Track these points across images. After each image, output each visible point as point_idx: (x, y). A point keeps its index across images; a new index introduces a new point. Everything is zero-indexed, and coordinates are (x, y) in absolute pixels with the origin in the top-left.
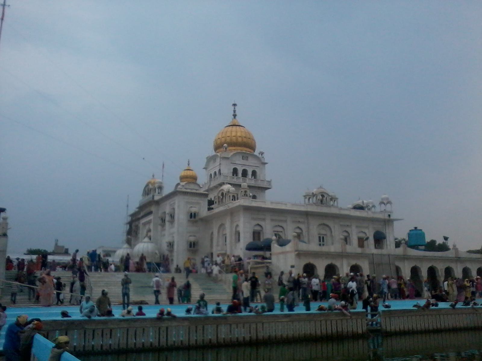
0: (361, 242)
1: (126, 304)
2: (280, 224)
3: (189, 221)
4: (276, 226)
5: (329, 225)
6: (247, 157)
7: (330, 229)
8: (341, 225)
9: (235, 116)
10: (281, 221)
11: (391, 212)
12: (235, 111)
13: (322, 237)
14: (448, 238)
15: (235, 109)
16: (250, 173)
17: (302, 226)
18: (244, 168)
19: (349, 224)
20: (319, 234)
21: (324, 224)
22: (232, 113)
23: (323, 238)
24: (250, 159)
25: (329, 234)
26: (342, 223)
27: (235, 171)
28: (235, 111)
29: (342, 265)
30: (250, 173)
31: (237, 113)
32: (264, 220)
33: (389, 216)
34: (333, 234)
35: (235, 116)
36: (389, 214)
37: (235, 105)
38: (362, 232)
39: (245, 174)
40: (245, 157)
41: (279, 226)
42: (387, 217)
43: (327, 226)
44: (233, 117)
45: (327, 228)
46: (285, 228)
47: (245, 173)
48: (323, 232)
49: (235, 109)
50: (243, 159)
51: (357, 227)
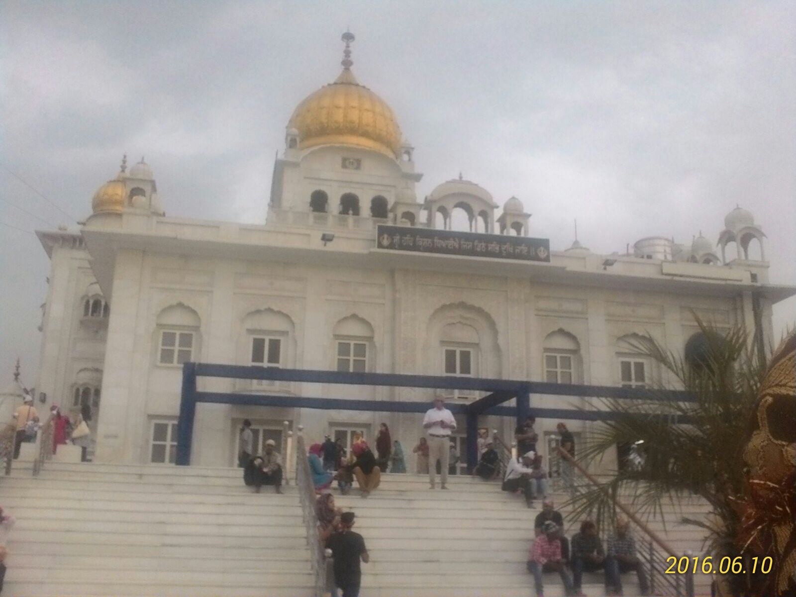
3: (82, 322)
4: (258, 312)
5: (487, 310)
7: (492, 325)
9: (347, 64)
11: (762, 266)
12: (347, 53)
13: (462, 353)
15: (348, 46)
16: (365, 206)
18: (347, 190)
20: (443, 343)
21: (463, 305)
23: (466, 356)
24: (367, 164)
25: (486, 342)
26: (543, 304)
27: (319, 202)
28: (347, 53)
30: (365, 206)
31: (353, 57)
34: (501, 341)
35: (347, 64)
39: (350, 204)
40: (352, 161)
43: (480, 311)
47: (350, 204)
48: (464, 335)
49: (348, 46)
50: (344, 166)
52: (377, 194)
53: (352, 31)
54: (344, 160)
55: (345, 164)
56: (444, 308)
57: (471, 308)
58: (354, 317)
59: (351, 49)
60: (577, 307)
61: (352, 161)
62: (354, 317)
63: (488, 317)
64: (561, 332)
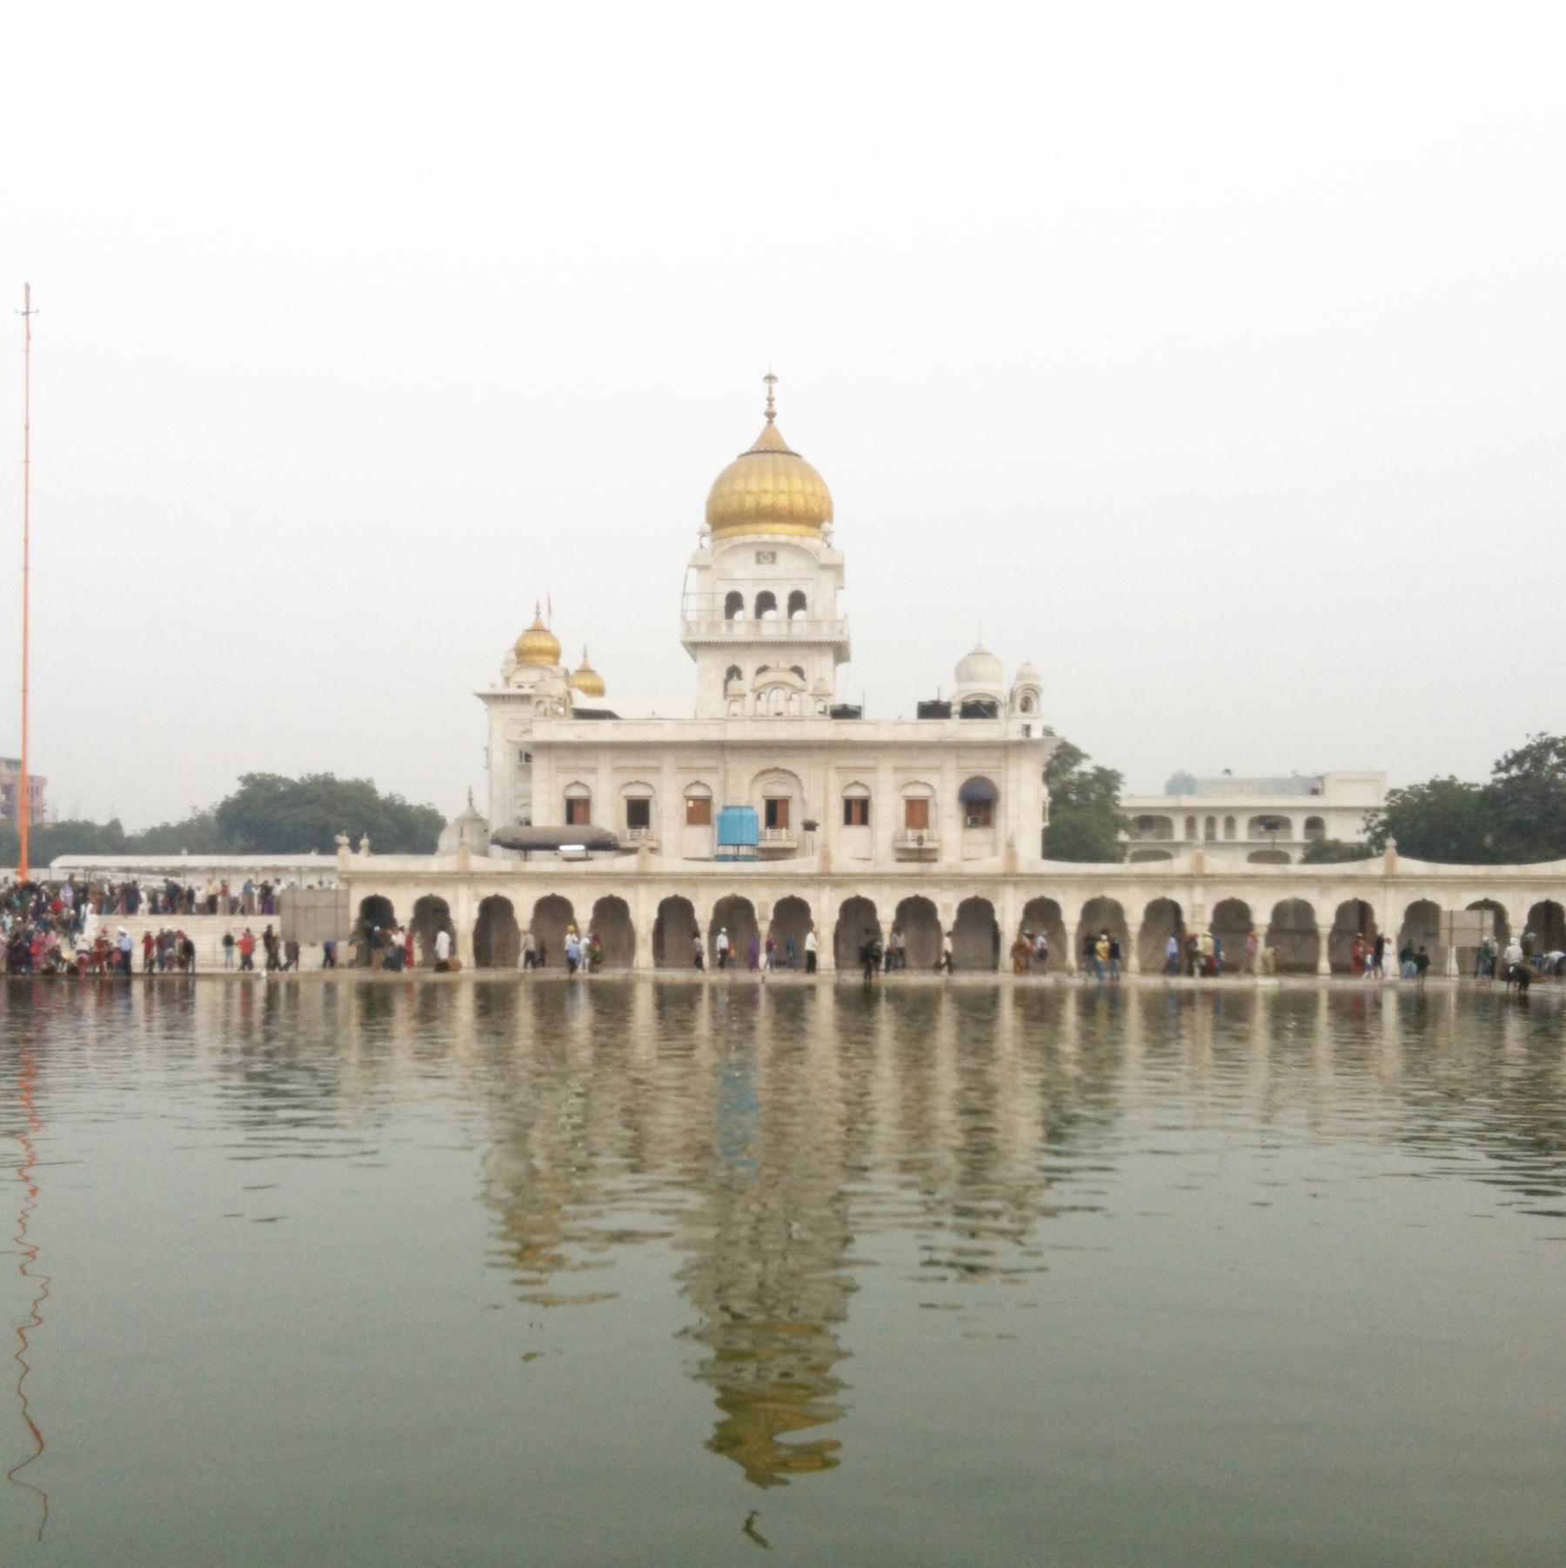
0: (917, 812)
1: (137, 975)
2: (641, 778)
4: (630, 784)
6: (773, 555)
8: (838, 768)
9: (770, 415)
10: (645, 769)
12: (770, 400)
14: (818, 825)
15: (770, 393)
17: (706, 778)
18: (762, 588)
19: (871, 763)
21: (776, 770)
22: (764, 406)
24: (784, 559)
26: (842, 763)
28: (770, 400)
29: (457, 898)
31: (777, 407)
32: (593, 770)
33: (1027, 729)
36: (1027, 722)
37: (770, 378)
38: (917, 782)
41: (638, 782)
42: (1015, 735)
43: (790, 773)
44: (767, 419)
45: (793, 780)
46: (656, 787)
47: (766, 601)
48: (778, 791)
49: (770, 393)
50: (758, 561)
51: (897, 769)
52: (794, 589)
53: (775, 373)
54: (758, 555)
55: (759, 558)
56: (763, 773)
57: (784, 771)
58: (697, 783)
59: (775, 394)
60: (871, 763)
61: (766, 555)
62: (697, 783)
63: (795, 776)
64: (857, 783)
